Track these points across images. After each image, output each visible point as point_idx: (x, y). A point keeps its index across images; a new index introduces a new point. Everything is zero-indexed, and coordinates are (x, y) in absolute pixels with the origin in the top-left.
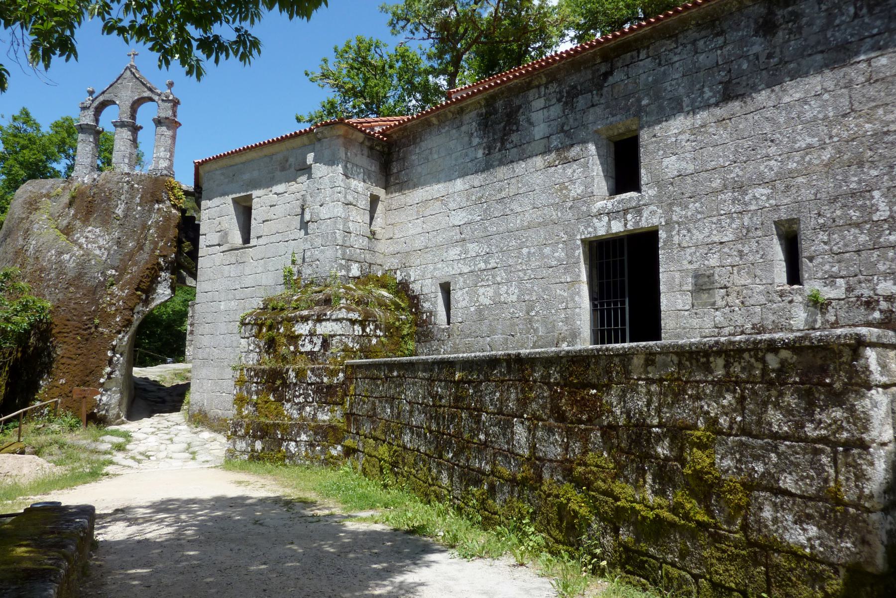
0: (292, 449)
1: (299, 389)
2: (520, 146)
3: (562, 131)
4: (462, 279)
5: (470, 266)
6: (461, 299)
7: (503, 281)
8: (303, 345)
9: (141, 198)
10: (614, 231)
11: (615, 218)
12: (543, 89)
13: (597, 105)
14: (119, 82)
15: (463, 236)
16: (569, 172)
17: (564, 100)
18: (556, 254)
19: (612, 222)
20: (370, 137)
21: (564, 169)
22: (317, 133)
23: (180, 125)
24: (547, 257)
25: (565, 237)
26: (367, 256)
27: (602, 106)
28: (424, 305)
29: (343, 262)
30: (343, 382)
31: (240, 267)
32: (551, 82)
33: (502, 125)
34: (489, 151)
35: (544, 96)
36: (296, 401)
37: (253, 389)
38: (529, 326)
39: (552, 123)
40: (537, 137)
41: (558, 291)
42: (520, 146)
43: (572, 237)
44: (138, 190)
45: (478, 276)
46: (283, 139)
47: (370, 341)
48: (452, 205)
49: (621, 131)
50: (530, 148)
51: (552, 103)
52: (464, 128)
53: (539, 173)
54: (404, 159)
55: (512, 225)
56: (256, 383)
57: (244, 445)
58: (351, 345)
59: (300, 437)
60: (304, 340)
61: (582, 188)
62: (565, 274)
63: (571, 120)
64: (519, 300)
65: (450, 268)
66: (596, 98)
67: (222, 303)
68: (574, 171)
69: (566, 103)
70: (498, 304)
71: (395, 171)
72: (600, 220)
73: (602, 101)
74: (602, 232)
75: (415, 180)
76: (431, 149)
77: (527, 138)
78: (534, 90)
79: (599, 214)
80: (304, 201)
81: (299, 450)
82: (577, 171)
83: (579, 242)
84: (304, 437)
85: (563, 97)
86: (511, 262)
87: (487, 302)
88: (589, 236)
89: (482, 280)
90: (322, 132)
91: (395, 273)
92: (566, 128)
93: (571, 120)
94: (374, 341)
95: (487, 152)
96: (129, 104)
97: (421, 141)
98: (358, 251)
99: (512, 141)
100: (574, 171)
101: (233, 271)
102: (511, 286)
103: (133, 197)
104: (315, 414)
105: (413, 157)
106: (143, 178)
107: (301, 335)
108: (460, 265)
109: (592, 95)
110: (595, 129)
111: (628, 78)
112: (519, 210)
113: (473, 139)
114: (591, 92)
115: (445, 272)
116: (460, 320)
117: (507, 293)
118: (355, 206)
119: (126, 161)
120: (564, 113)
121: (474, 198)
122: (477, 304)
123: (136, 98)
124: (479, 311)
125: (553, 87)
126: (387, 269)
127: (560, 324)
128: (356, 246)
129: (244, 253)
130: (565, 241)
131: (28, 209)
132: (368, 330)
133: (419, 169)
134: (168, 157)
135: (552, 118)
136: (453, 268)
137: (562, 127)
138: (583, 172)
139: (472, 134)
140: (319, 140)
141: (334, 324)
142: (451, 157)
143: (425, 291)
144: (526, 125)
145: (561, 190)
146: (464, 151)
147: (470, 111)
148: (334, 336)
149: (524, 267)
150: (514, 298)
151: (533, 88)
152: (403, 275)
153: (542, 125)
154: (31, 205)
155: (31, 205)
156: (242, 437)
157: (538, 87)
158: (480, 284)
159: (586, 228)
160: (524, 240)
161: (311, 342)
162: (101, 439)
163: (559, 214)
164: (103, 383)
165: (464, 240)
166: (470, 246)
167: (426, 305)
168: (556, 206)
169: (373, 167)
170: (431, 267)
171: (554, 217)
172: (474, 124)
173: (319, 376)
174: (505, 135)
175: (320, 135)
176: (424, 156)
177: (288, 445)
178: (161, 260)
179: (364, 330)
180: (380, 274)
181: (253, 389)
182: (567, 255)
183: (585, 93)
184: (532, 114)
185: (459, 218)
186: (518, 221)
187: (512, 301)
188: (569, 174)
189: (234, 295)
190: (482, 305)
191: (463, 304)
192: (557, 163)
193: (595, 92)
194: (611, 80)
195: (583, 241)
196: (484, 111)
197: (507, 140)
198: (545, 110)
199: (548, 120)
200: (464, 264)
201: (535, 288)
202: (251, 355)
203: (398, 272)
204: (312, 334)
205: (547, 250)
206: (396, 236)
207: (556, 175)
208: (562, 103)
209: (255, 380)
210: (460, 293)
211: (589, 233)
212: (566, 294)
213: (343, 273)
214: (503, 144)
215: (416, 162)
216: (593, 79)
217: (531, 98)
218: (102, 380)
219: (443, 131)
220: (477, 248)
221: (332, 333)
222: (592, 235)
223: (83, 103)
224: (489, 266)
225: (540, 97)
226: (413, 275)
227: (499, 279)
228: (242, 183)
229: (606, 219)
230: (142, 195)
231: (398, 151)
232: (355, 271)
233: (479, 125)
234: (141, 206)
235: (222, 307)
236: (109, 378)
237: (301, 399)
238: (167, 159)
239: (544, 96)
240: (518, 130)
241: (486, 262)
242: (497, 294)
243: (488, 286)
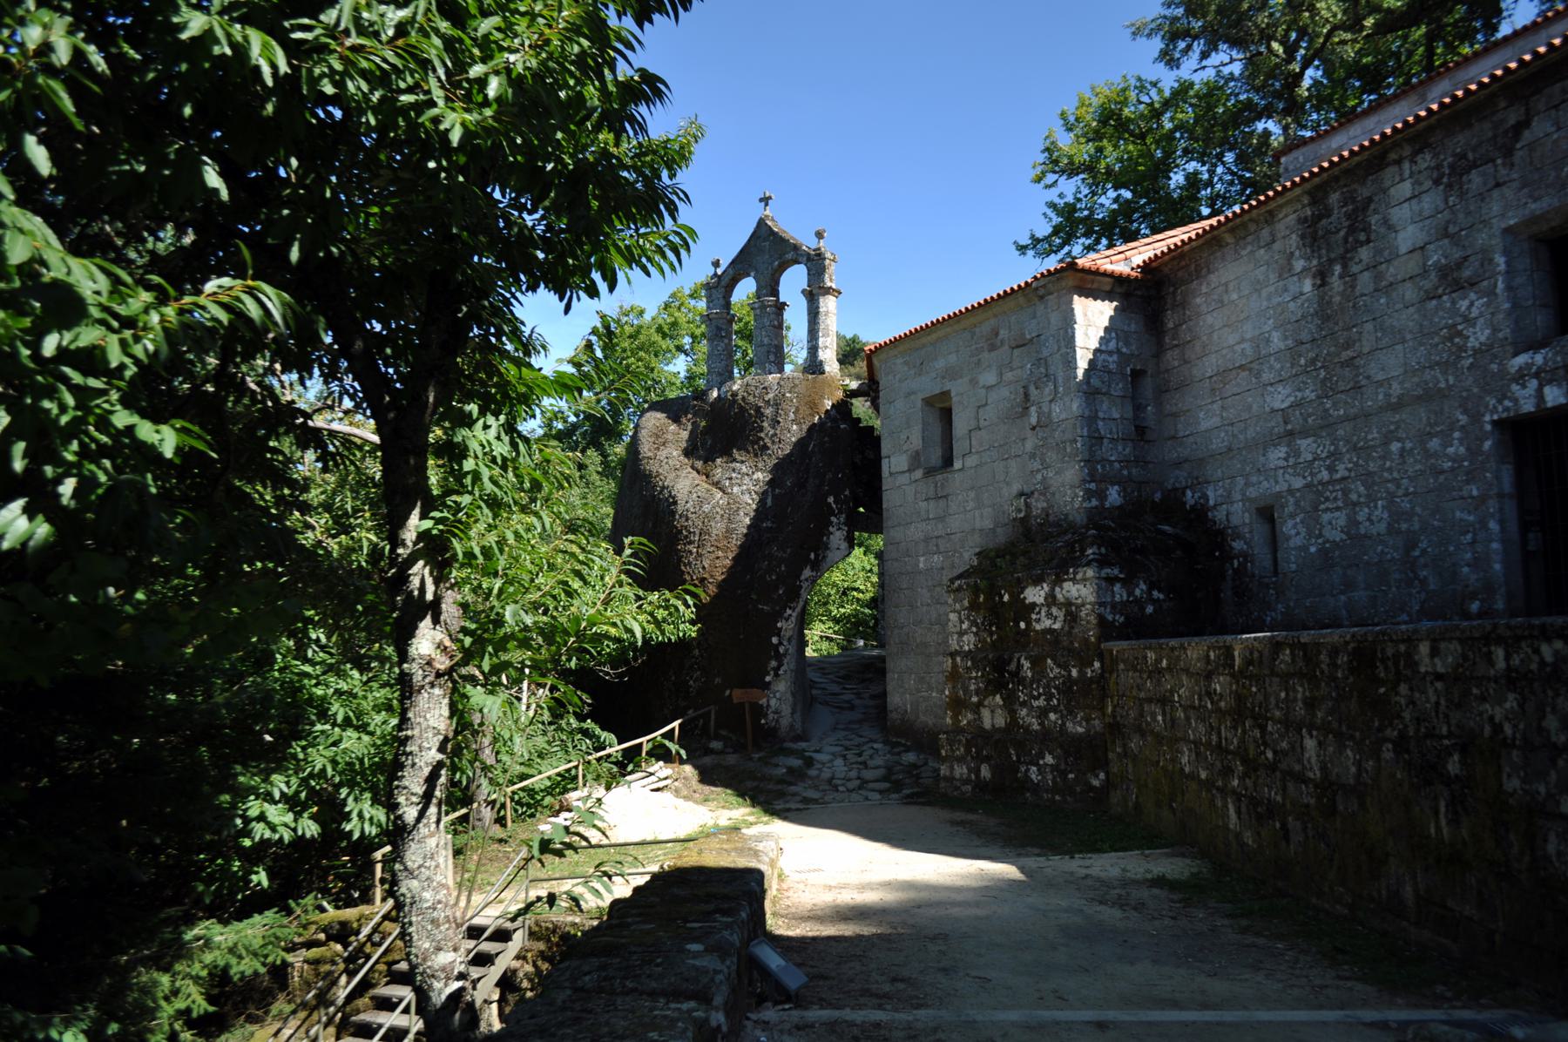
0: (1033, 776)
1: (1038, 687)
2: (1375, 267)
3: (1446, 235)
4: (1292, 500)
5: (1304, 477)
6: (1293, 532)
7: (1362, 500)
8: (1038, 621)
10: (1549, 405)
11: (1550, 382)
12: (1406, 165)
13: (1505, 183)
15: (1289, 427)
16: (1464, 304)
17: (1445, 180)
18: (1451, 450)
19: (1547, 390)
20: (1119, 279)
21: (1454, 303)
22: (1037, 289)
24: (1435, 455)
25: (1463, 419)
26: (1134, 470)
27: (1515, 184)
28: (1234, 544)
29: (1093, 486)
30: (1102, 675)
31: (942, 503)
32: (1420, 151)
33: (1342, 233)
34: (1323, 279)
35: (1410, 177)
36: (1035, 703)
37: (973, 687)
38: (1411, 575)
39: (1427, 222)
40: (1403, 249)
41: (1458, 514)
42: (1375, 267)
43: (1476, 418)
45: (1320, 494)
46: (987, 304)
47: (1143, 609)
48: (1267, 376)
49: (1553, 224)
50: (1392, 270)
51: (1425, 187)
52: (1277, 246)
53: (1411, 310)
54: (1184, 305)
55: (1370, 403)
56: (976, 678)
57: (965, 771)
58: (1110, 618)
59: (1043, 758)
60: (1039, 613)
61: (1487, 332)
62: (1468, 482)
63: (1461, 216)
64: (1391, 530)
65: (1272, 481)
66: (1503, 171)
67: (922, 559)
68: (1472, 304)
69: (1450, 186)
70: (1354, 536)
71: (1171, 325)
72: (1524, 386)
73: (1515, 176)
74: (1528, 407)
75: (1205, 338)
76: (1226, 284)
77: (1386, 253)
78: (1392, 169)
79: (1521, 377)
80: (1026, 395)
81: (1044, 777)
82: (1476, 303)
83: (1488, 427)
84: (1049, 759)
85: (1443, 175)
86: (1372, 466)
87: (1337, 536)
88: (1505, 415)
89: (1327, 499)
90: (1044, 286)
91: (1184, 494)
92: (1452, 229)
93: (1461, 216)
94: (1150, 609)
95: (1319, 282)
97: (1209, 272)
98: (1117, 465)
99: (1361, 261)
100: (1472, 304)
101: (933, 508)
102: (1376, 507)
104: (1064, 724)
105: (1198, 300)
107: (1034, 605)
108: (1287, 476)
109: (1496, 166)
110: (1503, 226)
111: (1559, 129)
112: (1381, 376)
113: (1294, 263)
114: (1493, 161)
115: (1262, 488)
116: (1294, 567)
117: (1369, 519)
118: (1104, 394)
120: (1447, 203)
121: (1303, 361)
122: (1320, 541)
124: (1323, 552)
125: (1425, 160)
126: (1170, 487)
127: (1466, 570)
128: (1113, 458)
130: (1463, 427)
132: (1138, 592)
133: (1210, 319)
135: (1426, 214)
136: (1277, 482)
137: (1446, 229)
138: (1488, 305)
139: (1292, 254)
140: (1042, 298)
141: (1080, 587)
142: (1260, 296)
143: (1235, 520)
144: (1382, 230)
145: (1451, 339)
146: (1281, 283)
147: (1286, 216)
148: (1083, 605)
149: (1395, 475)
150: (1382, 527)
151: (1388, 165)
152: (1197, 495)
153: (1411, 228)
154: (658, 437)
155: (658, 437)
156: (961, 760)
157: (1398, 162)
158: (1322, 507)
159: (1500, 401)
160: (1392, 427)
161: (1049, 615)
162: (774, 760)
163: (1451, 380)
164: (769, 683)
165: (1291, 434)
166: (1303, 443)
167: (1238, 545)
168: (1445, 366)
169: (1133, 326)
170: (1240, 481)
171: (1442, 385)
172: (1294, 236)
173: (1065, 666)
174: (1347, 251)
175: (1041, 292)
176: (1215, 297)
177: (1028, 770)
178: (831, 500)
179: (1130, 593)
180: (1158, 496)
181: (973, 687)
182: (1468, 449)
183: (1481, 165)
184: (1392, 211)
185: (1281, 398)
186: (1381, 397)
187: (1379, 534)
188: (1463, 308)
189: (937, 545)
190: (1328, 541)
191: (1297, 541)
192: (1440, 291)
193: (1499, 161)
194: (1527, 135)
195: (1494, 423)
196: (1309, 213)
197: (1351, 259)
198: (1414, 201)
199: (1419, 218)
200: (1296, 475)
201: (1418, 510)
202: (965, 638)
203: (1189, 493)
204: (1051, 600)
205: (1434, 444)
206: (1181, 434)
207: (1441, 313)
208: (1441, 187)
209: (974, 674)
210: (1290, 523)
211: (1507, 409)
212: (1471, 518)
213: (1094, 502)
214: (1345, 266)
215: (1204, 308)
216: (1495, 137)
217: (1387, 183)
218: (768, 679)
219: (1244, 253)
220: (1315, 445)
221: (1079, 601)
222: (1512, 414)
224: (1338, 476)
225: (1402, 180)
226: (1212, 496)
227: (1354, 497)
228: (934, 375)
229: (1534, 383)
231: (1174, 293)
232: (1114, 496)
233: (1303, 237)
235: (921, 565)
236: (777, 675)
237: (1041, 702)
239: (1410, 177)
240: (1368, 241)
241: (1331, 469)
242: (1353, 522)
243: (1338, 509)
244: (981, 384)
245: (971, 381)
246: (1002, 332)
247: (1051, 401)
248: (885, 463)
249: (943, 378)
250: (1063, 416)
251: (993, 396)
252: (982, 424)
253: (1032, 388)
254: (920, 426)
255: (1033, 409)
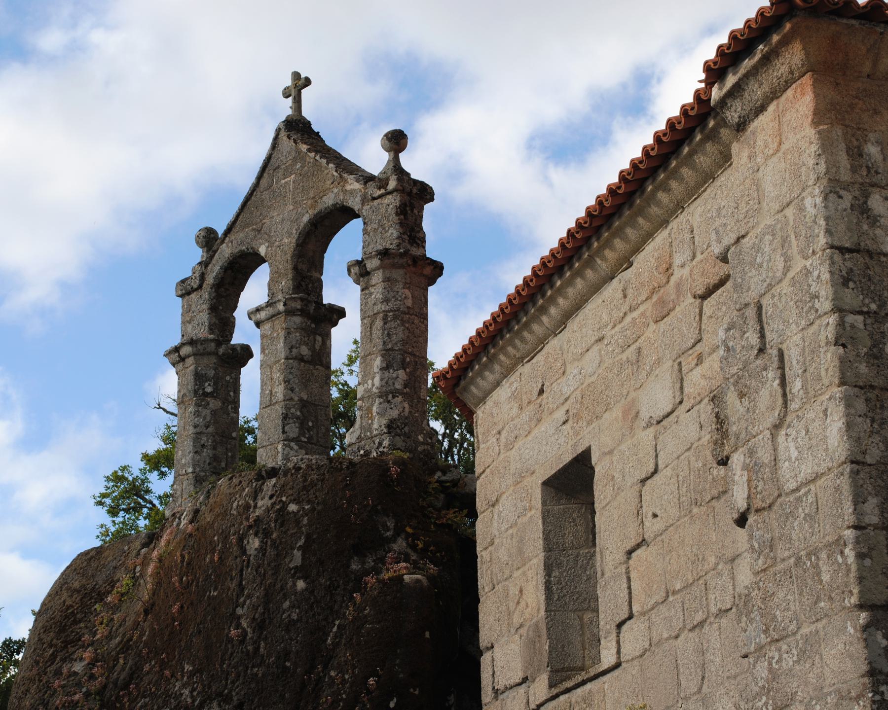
9: (304, 549)
14: (264, 182)
23: (437, 269)
44: (298, 522)
80: (720, 421)
96: (289, 242)
103: (282, 550)
106: (314, 476)
119: (293, 430)
123: (306, 218)
129: (587, 700)
131: (51, 646)
134: (398, 386)
140: (741, 127)
155: (62, 630)
223: (183, 281)
228: (560, 415)
230: (308, 537)
234: (305, 578)
238: (395, 393)
244: (644, 415)
245: (625, 413)
246: (678, 260)
247: (777, 427)
248: (485, 660)
249: (578, 417)
250: (806, 470)
251: (670, 446)
252: (652, 527)
253: (731, 397)
254: (542, 555)
255: (737, 460)
